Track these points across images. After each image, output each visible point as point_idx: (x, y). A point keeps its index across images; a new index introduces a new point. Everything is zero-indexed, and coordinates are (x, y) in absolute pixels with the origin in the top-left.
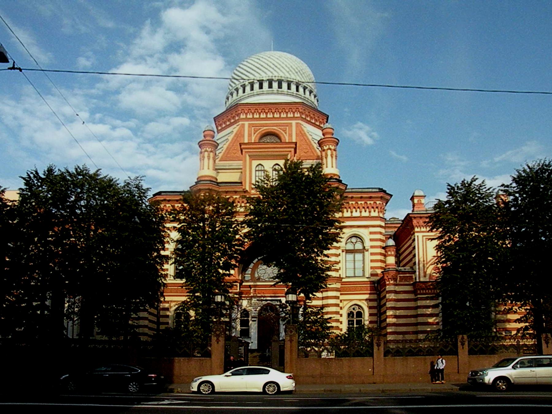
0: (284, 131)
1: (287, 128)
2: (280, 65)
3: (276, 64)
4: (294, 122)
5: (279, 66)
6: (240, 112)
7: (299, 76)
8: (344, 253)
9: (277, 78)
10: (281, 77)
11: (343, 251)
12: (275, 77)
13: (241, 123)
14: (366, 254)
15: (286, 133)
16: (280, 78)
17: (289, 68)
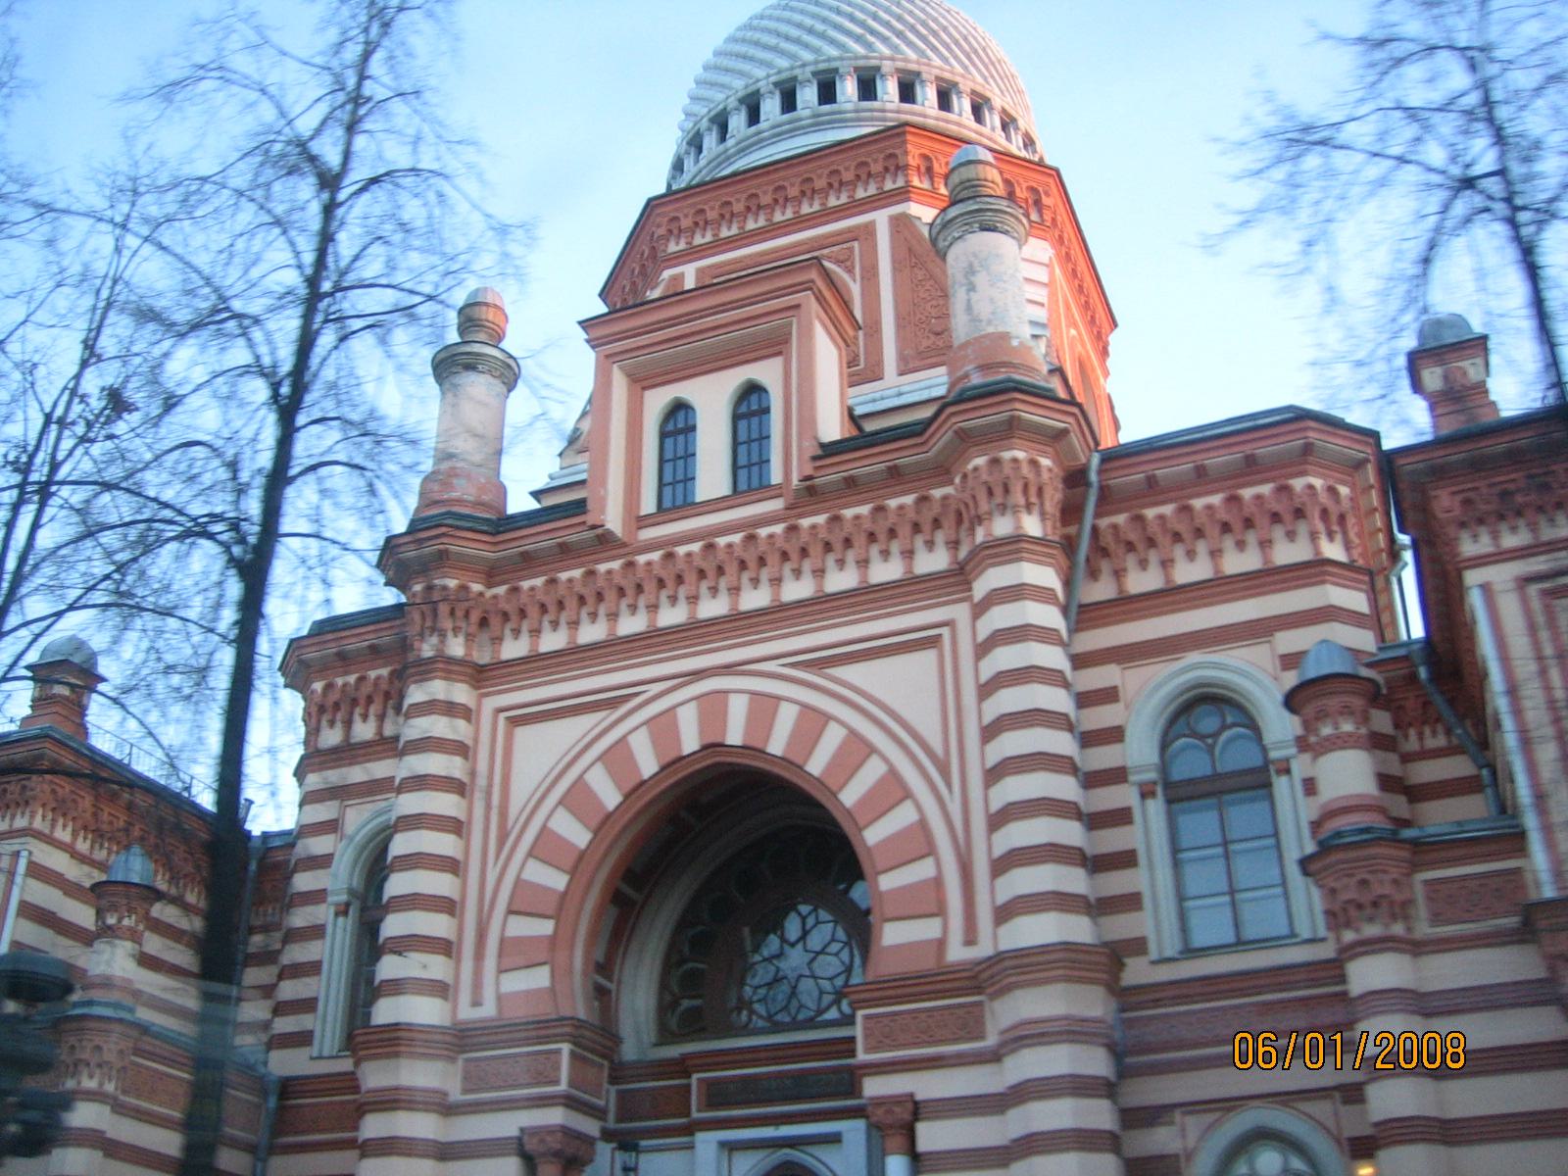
0: (838, 262)
1: (856, 244)
2: (824, 20)
3: (808, 22)
4: (881, 218)
5: (820, 27)
6: (662, 231)
7: (910, 44)
8: (1156, 807)
9: (809, 69)
10: (829, 60)
11: (1146, 793)
12: (804, 65)
13: (667, 274)
14: (1281, 784)
15: (850, 271)
16: (822, 66)
17: (862, 24)
